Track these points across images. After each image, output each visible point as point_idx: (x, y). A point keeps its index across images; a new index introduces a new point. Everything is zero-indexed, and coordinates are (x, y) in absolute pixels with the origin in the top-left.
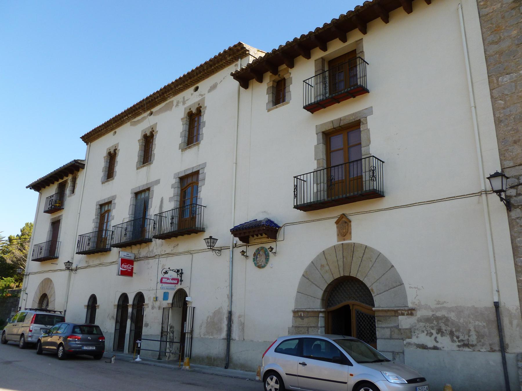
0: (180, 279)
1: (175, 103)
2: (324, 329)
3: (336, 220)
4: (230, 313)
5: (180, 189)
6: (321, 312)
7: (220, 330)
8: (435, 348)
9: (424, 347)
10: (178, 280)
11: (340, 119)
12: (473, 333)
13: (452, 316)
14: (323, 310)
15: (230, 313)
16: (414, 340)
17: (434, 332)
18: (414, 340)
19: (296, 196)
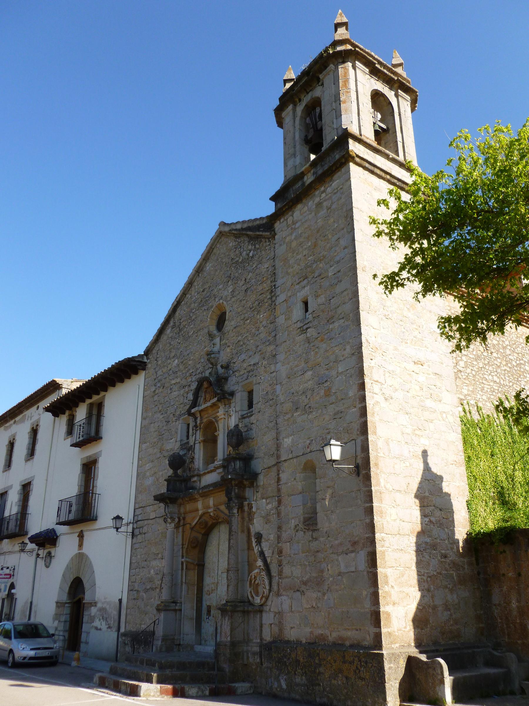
0: (12, 574)
1: (27, 417)
2: (68, 616)
3: (77, 534)
4: (31, 603)
5: (22, 495)
6: (66, 603)
7: (26, 617)
8: (100, 629)
9: (96, 628)
10: (10, 575)
11: (90, 457)
12: (112, 619)
13: (108, 607)
14: (68, 601)
15: (31, 603)
16: (95, 624)
17: (101, 618)
18: (95, 624)
19: (58, 515)
